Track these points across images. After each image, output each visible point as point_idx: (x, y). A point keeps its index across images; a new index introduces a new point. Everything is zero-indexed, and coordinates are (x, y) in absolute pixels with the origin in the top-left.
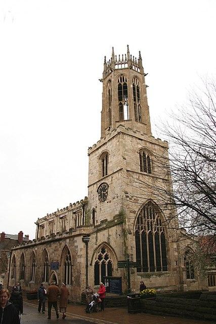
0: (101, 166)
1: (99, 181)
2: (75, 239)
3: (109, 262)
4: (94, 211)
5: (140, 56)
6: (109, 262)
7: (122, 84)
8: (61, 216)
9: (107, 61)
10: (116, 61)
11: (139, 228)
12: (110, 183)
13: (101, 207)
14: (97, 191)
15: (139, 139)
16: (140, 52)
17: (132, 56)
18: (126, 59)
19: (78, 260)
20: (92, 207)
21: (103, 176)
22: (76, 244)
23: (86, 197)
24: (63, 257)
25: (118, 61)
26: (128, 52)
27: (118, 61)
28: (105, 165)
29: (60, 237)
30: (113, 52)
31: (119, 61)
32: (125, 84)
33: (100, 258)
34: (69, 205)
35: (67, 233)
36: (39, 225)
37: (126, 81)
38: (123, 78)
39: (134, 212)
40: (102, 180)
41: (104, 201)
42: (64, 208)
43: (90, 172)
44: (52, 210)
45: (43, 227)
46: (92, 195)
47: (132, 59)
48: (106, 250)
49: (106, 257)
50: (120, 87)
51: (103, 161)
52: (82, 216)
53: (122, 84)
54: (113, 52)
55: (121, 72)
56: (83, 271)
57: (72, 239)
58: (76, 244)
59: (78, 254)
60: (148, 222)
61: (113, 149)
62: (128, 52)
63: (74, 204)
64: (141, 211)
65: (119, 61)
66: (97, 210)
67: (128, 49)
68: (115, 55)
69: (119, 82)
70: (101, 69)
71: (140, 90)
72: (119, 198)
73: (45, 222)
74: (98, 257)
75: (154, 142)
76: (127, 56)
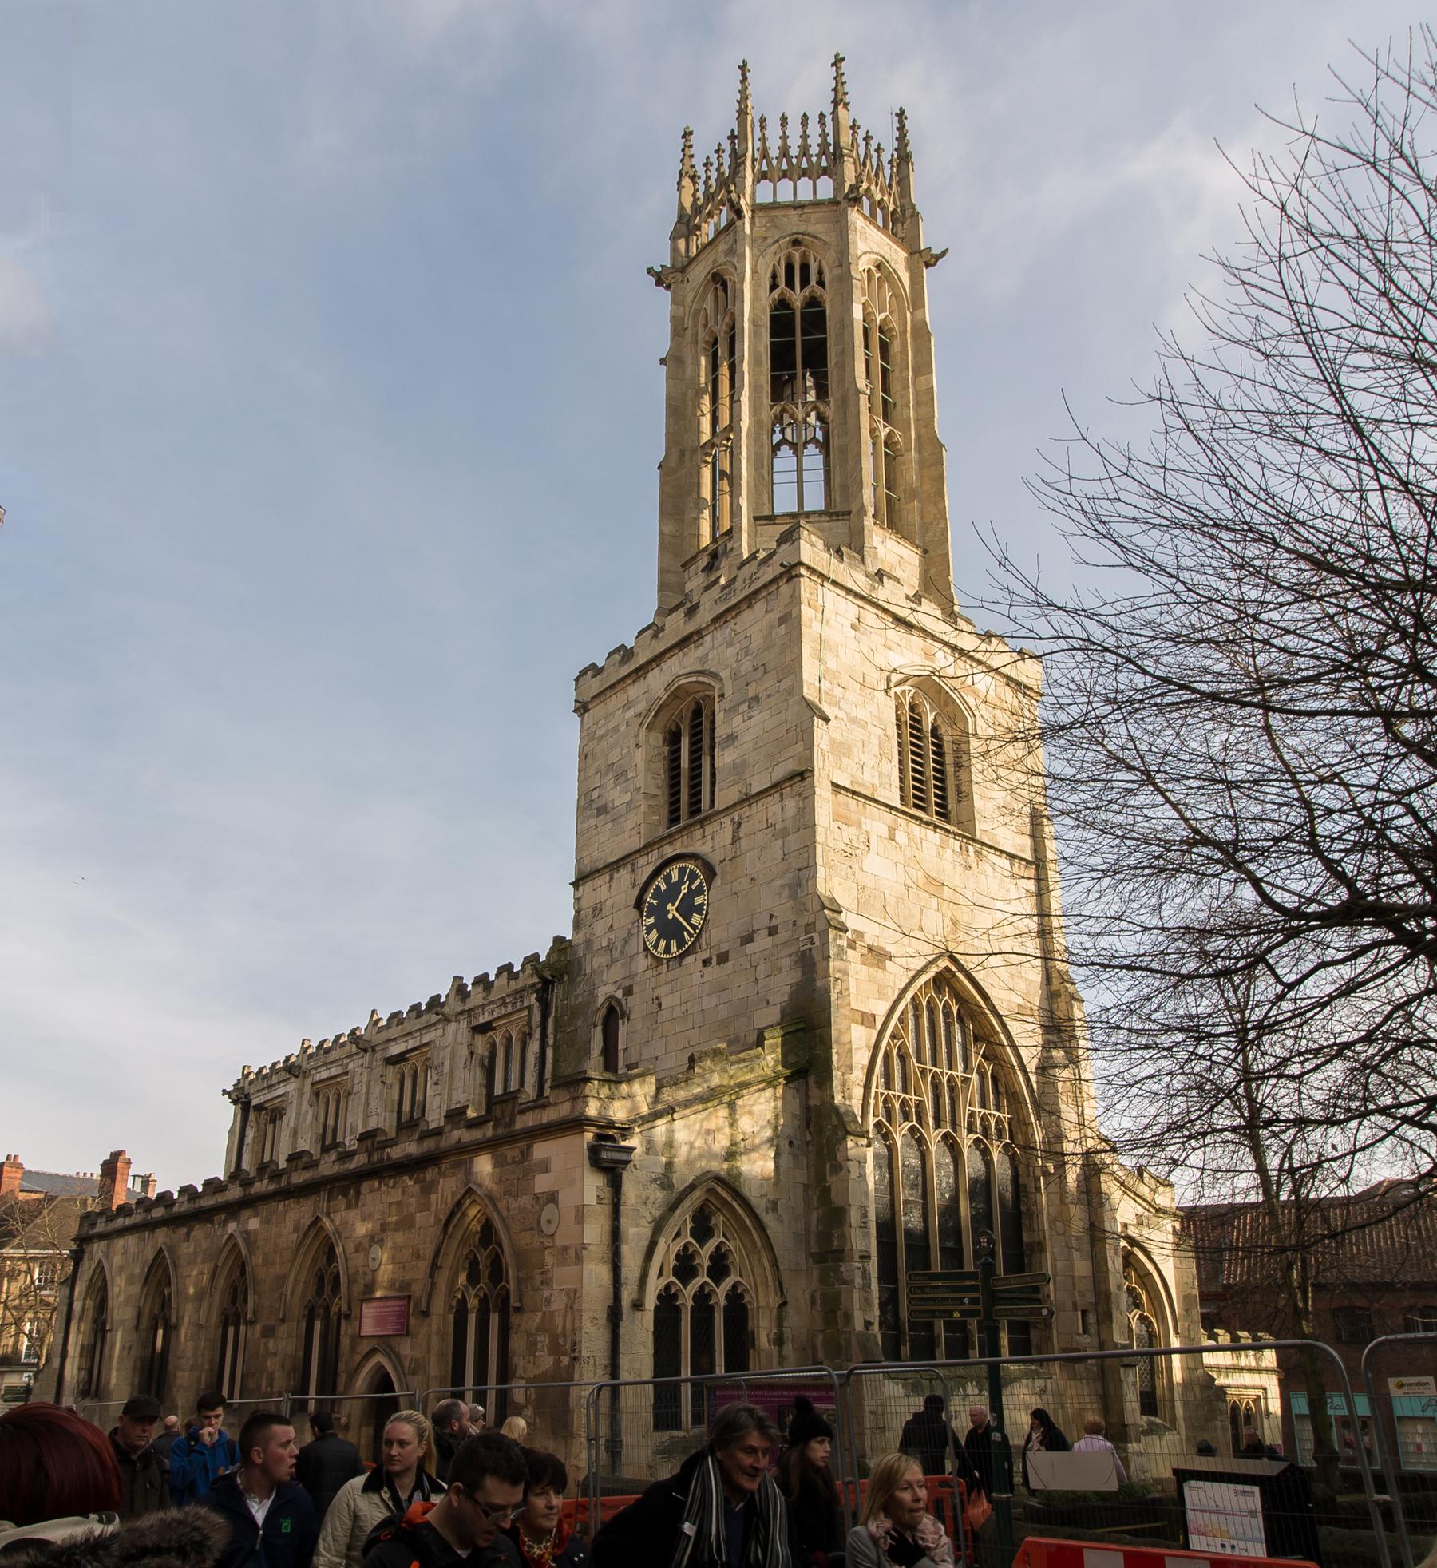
0: (661, 767)
1: (648, 847)
2: (541, 1150)
3: (735, 1298)
4: (613, 1014)
5: (902, 138)
6: (735, 1298)
7: (797, 298)
8: (395, 1049)
9: (698, 162)
11: (889, 1112)
12: (729, 852)
13: (662, 991)
14: (639, 904)
15: (899, 620)
16: (901, 115)
17: (861, 134)
18: (823, 146)
19: (562, 1275)
20: (603, 993)
21: (674, 819)
22: (542, 1183)
23: (558, 940)
24: (447, 1261)
28: (685, 763)
29: (429, 1145)
31: (784, 152)
33: (685, 1267)
34: (444, 989)
35: (473, 1124)
36: (254, 1102)
38: (805, 268)
39: (867, 1019)
40: (669, 838)
41: (682, 956)
42: (415, 1008)
43: (591, 807)
44: (349, 1019)
45: (274, 1114)
46: (600, 927)
48: (718, 1220)
49: (719, 1267)
50: (780, 320)
51: (673, 739)
52: (534, 1047)
53: (797, 298)
55: (793, 222)
56: (593, 1340)
57: (511, 1152)
58: (542, 1183)
59: (559, 1242)
60: (936, 1086)
61: (746, 666)
63: (482, 980)
64: (902, 1020)
66: (636, 1006)
69: (774, 286)
72: (783, 935)
73: (292, 1087)
74: (672, 1262)
75: (968, 643)
76: (829, 129)
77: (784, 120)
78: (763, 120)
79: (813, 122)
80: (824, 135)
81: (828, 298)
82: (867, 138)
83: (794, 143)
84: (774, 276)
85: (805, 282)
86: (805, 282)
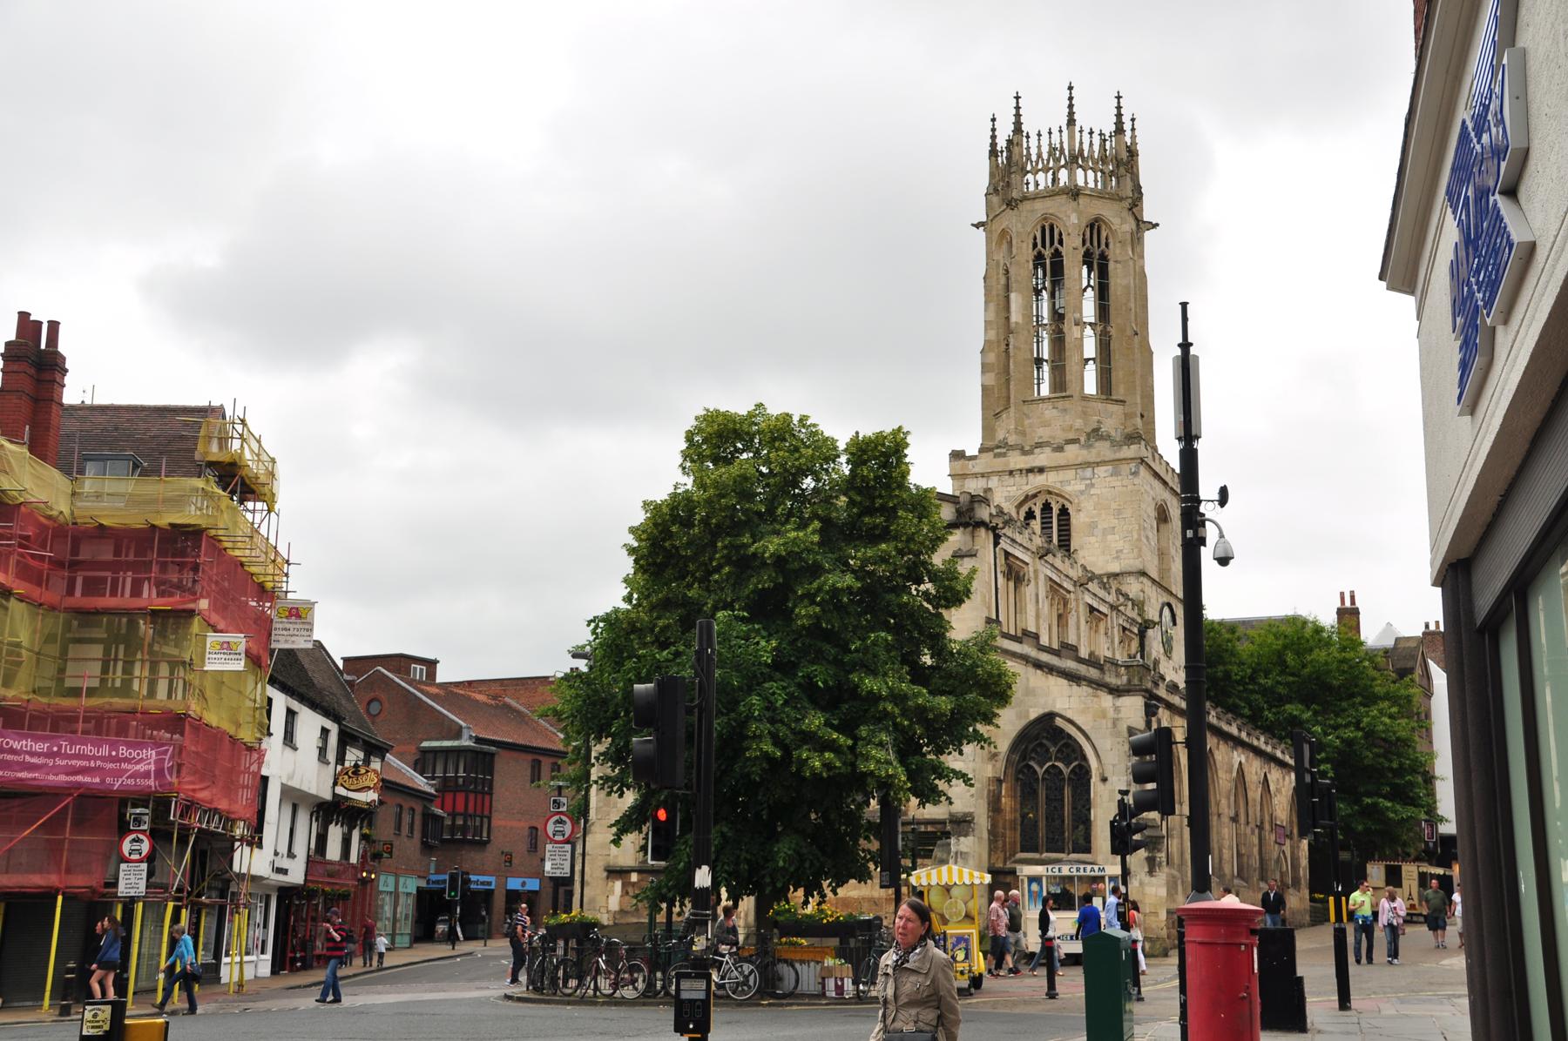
7: (1047, 253)
10: (1029, 154)
17: (1086, 131)
25: (1034, 158)
26: (1071, 122)
27: (1034, 158)
30: (1018, 115)
31: (1039, 155)
32: (1057, 254)
37: (1061, 242)
47: (1086, 147)
53: (1047, 253)
54: (1018, 115)
62: (1071, 122)
65: (1039, 155)
67: (1071, 106)
68: (1024, 128)
69: (1035, 245)
70: (980, 175)
71: (1111, 266)
77: (1039, 135)
81: (1063, 250)
82: (1091, 133)
85: (1052, 243)
86: (1052, 243)
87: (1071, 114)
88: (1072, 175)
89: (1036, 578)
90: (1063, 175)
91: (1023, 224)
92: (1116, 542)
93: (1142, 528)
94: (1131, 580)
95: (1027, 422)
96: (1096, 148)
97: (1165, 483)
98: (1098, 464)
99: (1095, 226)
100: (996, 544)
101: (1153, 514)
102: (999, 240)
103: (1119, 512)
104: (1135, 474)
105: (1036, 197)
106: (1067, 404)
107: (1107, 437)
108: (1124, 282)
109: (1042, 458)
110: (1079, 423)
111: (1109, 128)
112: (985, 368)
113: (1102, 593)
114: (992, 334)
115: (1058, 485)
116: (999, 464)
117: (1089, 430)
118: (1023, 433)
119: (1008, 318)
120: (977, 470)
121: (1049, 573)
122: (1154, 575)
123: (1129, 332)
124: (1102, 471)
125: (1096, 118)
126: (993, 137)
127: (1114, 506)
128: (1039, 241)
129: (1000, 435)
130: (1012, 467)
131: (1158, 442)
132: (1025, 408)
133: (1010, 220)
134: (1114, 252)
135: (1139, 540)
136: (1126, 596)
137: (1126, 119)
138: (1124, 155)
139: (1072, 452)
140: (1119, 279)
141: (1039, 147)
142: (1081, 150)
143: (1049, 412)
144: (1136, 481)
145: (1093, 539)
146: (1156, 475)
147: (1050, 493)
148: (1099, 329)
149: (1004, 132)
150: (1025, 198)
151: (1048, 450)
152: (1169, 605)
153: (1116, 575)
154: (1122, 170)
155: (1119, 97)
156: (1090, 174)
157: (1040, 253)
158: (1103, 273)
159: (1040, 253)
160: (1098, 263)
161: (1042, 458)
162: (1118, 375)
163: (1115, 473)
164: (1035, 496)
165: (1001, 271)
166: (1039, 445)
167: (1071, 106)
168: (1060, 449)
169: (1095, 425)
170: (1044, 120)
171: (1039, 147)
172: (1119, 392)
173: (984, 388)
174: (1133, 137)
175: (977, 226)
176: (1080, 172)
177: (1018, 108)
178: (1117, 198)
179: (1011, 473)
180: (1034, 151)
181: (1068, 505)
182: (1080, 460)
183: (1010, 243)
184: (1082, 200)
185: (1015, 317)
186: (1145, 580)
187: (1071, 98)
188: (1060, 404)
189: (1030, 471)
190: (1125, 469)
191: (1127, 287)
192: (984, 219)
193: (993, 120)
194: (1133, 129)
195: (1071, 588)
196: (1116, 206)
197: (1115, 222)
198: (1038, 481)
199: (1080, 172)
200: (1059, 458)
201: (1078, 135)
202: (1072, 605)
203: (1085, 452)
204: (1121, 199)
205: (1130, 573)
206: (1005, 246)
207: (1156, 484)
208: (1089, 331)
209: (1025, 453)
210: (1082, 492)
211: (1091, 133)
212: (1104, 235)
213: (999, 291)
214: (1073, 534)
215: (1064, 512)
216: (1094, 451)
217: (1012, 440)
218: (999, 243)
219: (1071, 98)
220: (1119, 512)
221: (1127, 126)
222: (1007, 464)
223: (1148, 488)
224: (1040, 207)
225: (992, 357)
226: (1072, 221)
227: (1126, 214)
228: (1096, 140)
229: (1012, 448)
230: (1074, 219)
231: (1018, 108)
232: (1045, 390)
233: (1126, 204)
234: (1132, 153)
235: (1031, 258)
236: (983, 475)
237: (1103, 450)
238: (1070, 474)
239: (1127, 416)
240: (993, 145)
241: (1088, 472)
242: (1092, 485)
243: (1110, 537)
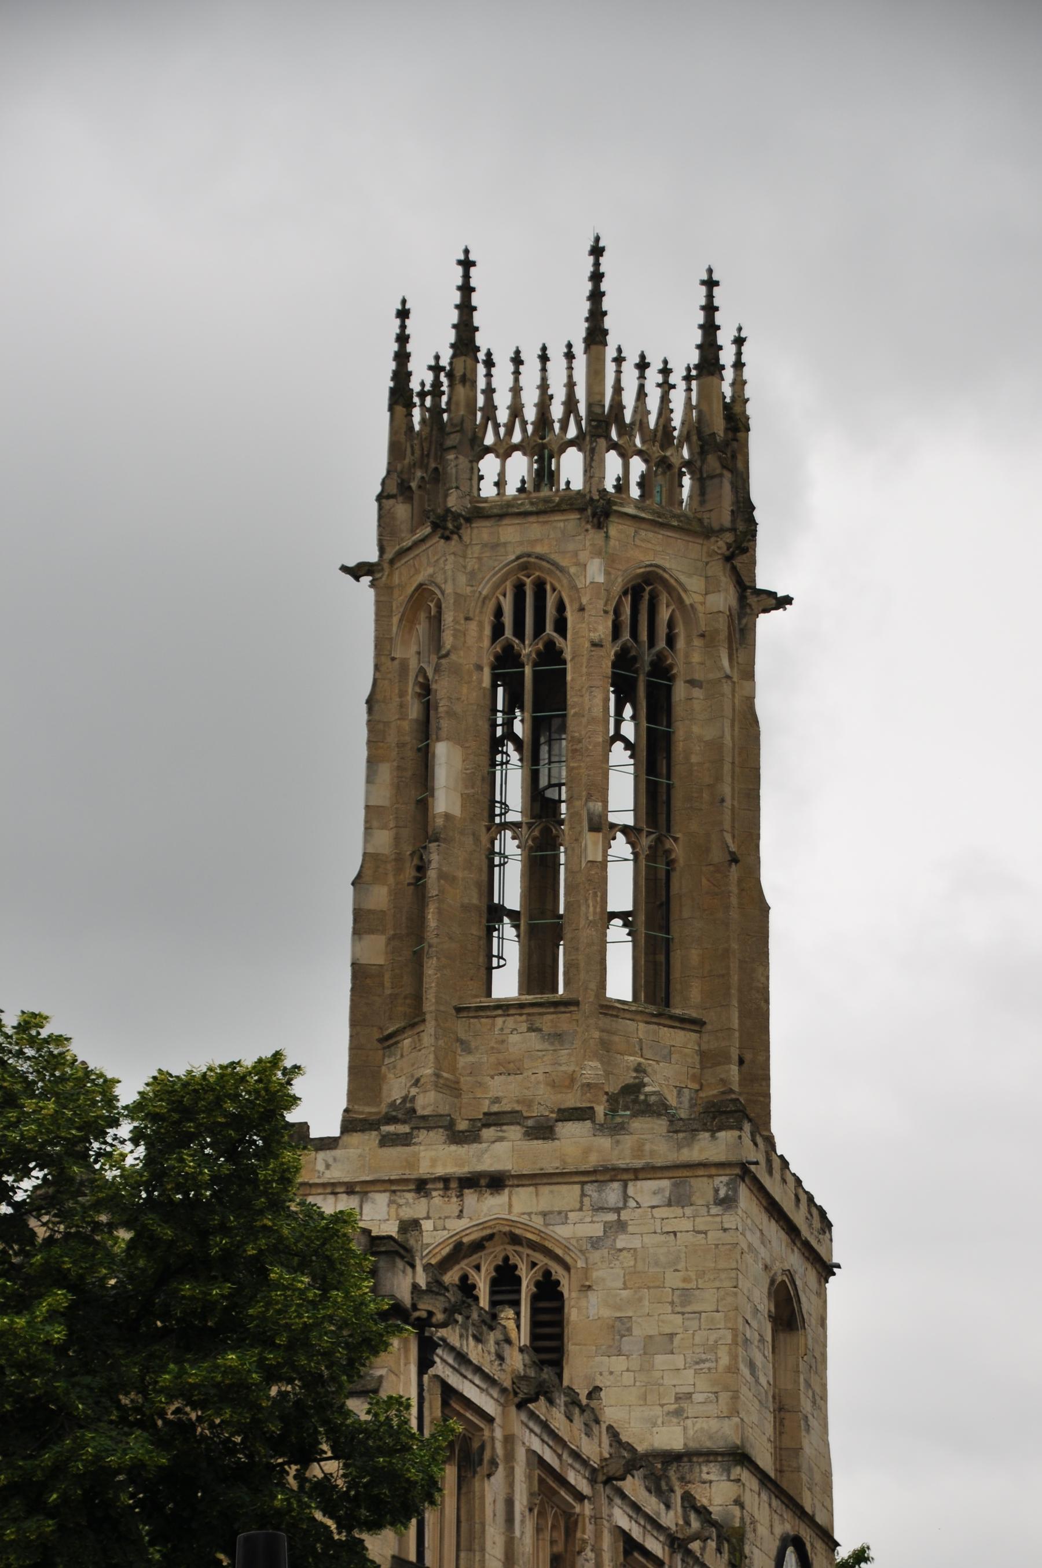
7: (528, 650)
10: (490, 408)
18: (571, 404)
25: (503, 416)
26: (596, 334)
27: (503, 416)
30: (466, 308)
31: (516, 410)
32: (551, 655)
37: (561, 626)
47: (629, 399)
53: (528, 650)
54: (466, 308)
62: (596, 334)
65: (516, 410)
67: (596, 296)
68: (482, 340)
69: (498, 630)
70: (365, 450)
71: (680, 691)
77: (517, 360)
78: (489, 363)
79: (557, 355)
80: (571, 385)
82: (642, 365)
83: (530, 398)
84: (499, 612)
87: (596, 317)
88: (593, 468)
89: (510, 1457)
90: (571, 468)
91: (468, 576)
92: (676, 1372)
93: (740, 1341)
94: (711, 1472)
95: (464, 1061)
96: (653, 403)
97: (791, 1229)
98: (638, 1173)
99: (644, 591)
100: (425, 1364)
101: (765, 1305)
102: (408, 609)
103: (686, 1295)
104: (727, 1202)
105: (503, 511)
106: (563, 1021)
107: (657, 1108)
108: (709, 733)
109: (500, 1152)
110: (592, 1070)
111: (686, 355)
112: (363, 922)
113: (651, 1504)
114: (384, 840)
115: (538, 1222)
116: (391, 1162)
117: (613, 1088)
118: (453, 1089)
119: (424, 805)
120: (336, 1174)
121: (536, 1445)
122: (765, 1460)
123: (717, 856)
124: (645, 1191)
125: (656, 330)
126: (402, 357)
127: (673, 1280)
128: (508, 619)
129: (395, 1089)
130: (424, 1169)
131: (777, 1127)
132: (461, 1027)
133: (444, 566)
134: (689, 657)
135: (733, 1369)
136: (703, 1513)
137: (725, 338)
138: (718, 426)
139: (575, 1142)
140: (694, 726)
141: (516, 390)
142: (618, 406)
143: (519, 1039)
144: (730, 1220)
145: (618, 1363)
146: (774, 1209)
147: (515, 1239)
148: (645, 842)
149: (432, 341)
150: (480, 512)
151: (514, 1132)
152: (797, 1543)
153: (671, 1458)
154: (712, 462)
155: (710, 284)
156: (638, 466)
157: (508, 648)
158: (658, 713)
159: (508, 648)
160: (645, 680)
161: (500, 1152)
162: (689, 957)
163: (678, 1199)
164: (478, 1246)
165: (411, 688)
166: (495, 1119)
167: (596, 296)
168: (542, 1131)
169: (630, 1078)
170: (528, 323)
171: (516, 390)
172: (690, 998)
173: (360, 973)
174: (739, 384)
175: (356, 572)
176: (613, 463)
177: (466, 289)
178: (696, 528)
179: (421, 1186)
180: (503, 400)
181: (558, 1272)
182: (593, 1161)
183: (436, 621)
184: (615, 529)
185: (446, 800)
186: (745, 1475)
187: (597, 277)
188: (548, 1021)
189: (470, 1182)
190: (703, 1188)
191: (715, 746)
192: (372, 556)
193: (403, 314)
194: (739, 365)
195: (583, 1486)
196: (695, 549)
197: (693, 586)
198: (488, 1209)
199: (613, 463)
200: (543, 1155)
201: (610, 368)
202: (587, 1532)
203: (605, 1142)
204: (708, 533)
205: (708, 1455)
206: (422, 628)
207: (773, 1230)
208: (621, 847)
209: (457, 1138)
210: (595, 1243)
211: (642, 365)
212: (664, 615)
213: (404, 732)
214: (572, 1348)
215: (549, 1292)
216: (628, 1141)
217: (427, 1102)
218: (409, 619)
219: (597, 277)
220: (686, 1295)
221: (727, 357)
222: (413, 1164)
223: (754, 1239)
224: (514, 538)
225: (380, 897)
226: (590, 573)
227: (718, 570)
228: (653, 377)
229: (427, 1123)
230: (595, 572)
231: (466, 289)
232: (506, 984)
233: (720, 545)
234: (736, 421)
235: (487, 660)
236: (350, 1189)
237: (649, 1139)
238: (567, 1195)
239: (708, 1059)
240: (401, 375)
241: (612, 1194)
242: (621, 1226)
243: (659, 1359)
